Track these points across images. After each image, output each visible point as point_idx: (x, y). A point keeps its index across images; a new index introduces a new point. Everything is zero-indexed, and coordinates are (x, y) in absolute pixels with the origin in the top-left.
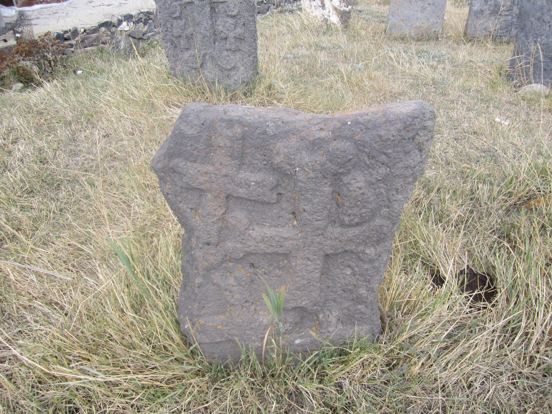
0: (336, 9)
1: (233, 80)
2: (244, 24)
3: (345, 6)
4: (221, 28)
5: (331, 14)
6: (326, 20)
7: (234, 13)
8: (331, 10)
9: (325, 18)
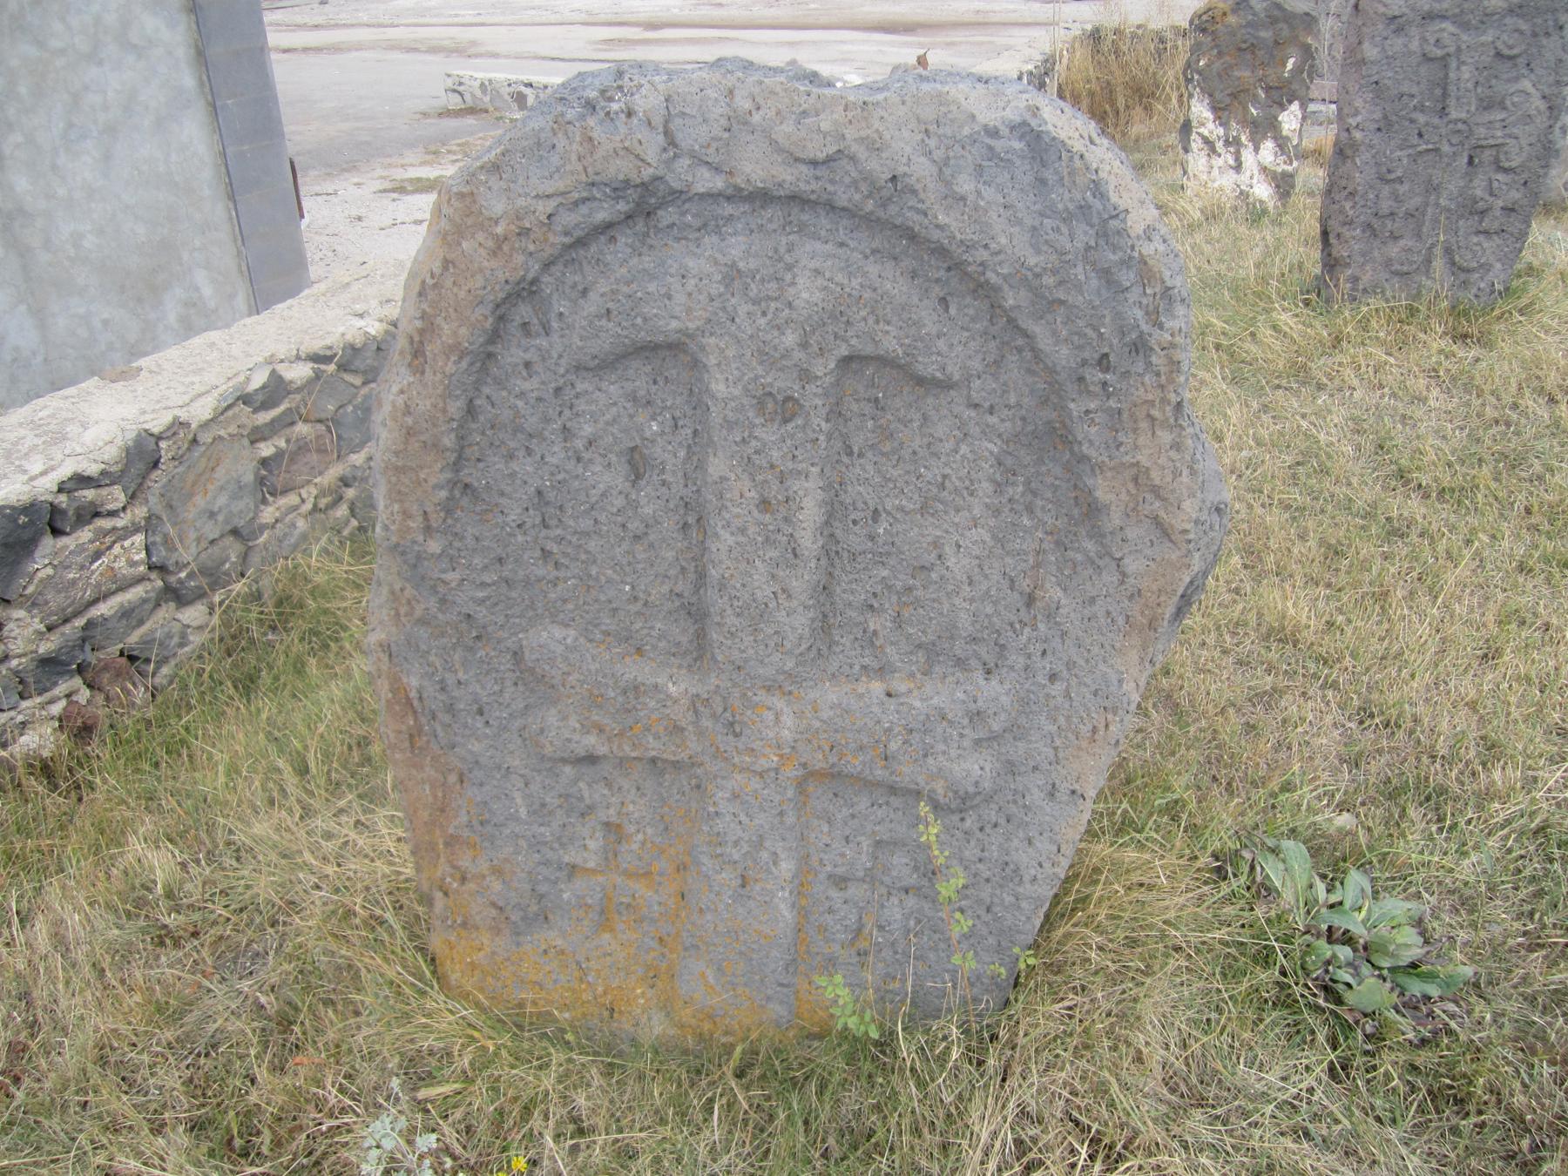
0: (1264, 169)
1: (1474, 291)
2: (1526, 183)
3: (1285, 163)
4: (1479, 193)
5: (1255, 181)
6: (1243, 195)
7: (1513, 164)
8: (1256, 172)
9: (1242, 193)
